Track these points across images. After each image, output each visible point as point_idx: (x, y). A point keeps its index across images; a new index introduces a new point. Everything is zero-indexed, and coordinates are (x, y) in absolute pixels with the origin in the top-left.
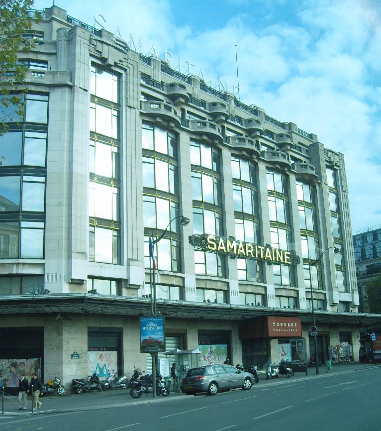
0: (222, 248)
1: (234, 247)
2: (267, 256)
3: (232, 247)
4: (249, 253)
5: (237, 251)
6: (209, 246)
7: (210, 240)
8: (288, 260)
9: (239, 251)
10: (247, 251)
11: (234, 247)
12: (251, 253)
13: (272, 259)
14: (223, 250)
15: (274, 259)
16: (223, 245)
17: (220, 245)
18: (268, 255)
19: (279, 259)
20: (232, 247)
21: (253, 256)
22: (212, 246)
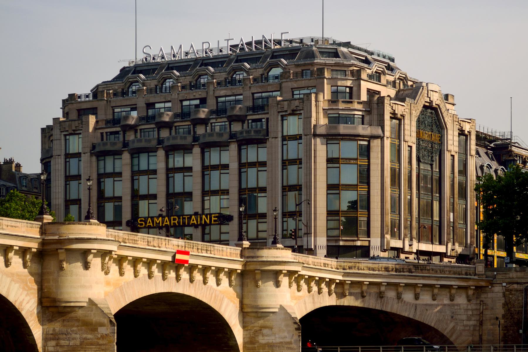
0: (149, 224)
1: (160, 222)
2: (192, 222)
3: (158, 222)
4: (175, 223)
5: (163, 223)
6: (139, 225)
7: (141, 221)
8: (214, 221)
9: (165, 223)
10: (172, 222)
11: (160, 222)
12: (176, 223)
13: (197, 222)
14: (151, 225)
15: (199, 223)
16: (151, 221)
17: (148, 222)
18: (193, 220)
19: (205, 221)
20: (158, 222)
21: (177, 225)
22: (142, 224)
